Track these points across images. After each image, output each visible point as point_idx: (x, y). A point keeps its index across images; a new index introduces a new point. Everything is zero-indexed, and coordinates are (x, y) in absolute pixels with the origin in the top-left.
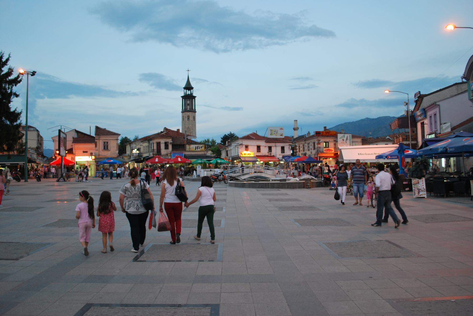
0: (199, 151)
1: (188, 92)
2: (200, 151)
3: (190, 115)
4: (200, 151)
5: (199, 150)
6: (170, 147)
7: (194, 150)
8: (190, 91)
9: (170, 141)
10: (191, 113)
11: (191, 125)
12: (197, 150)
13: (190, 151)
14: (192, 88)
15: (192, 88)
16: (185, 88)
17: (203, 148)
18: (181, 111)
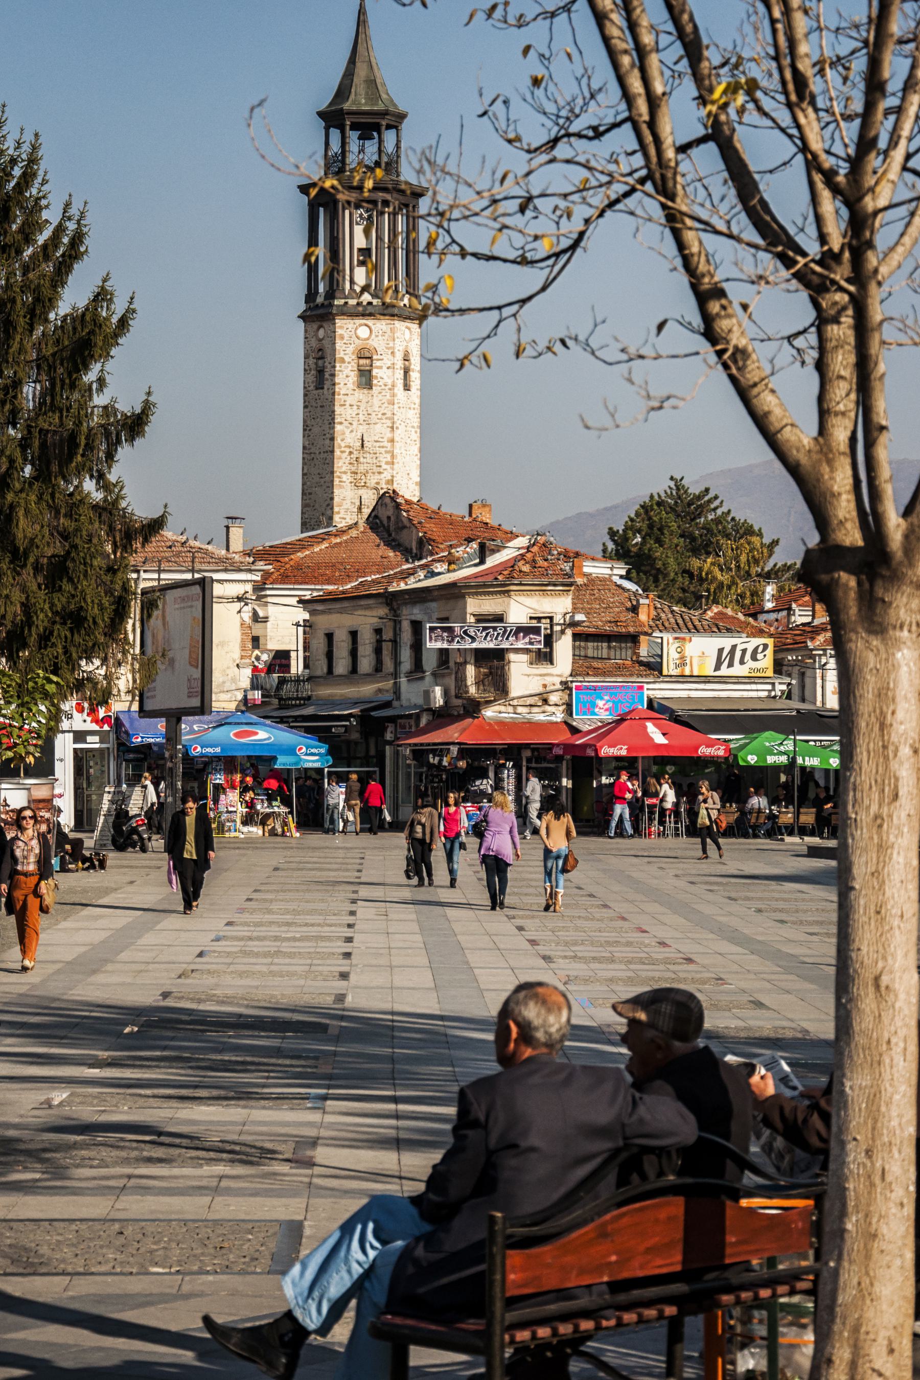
0: (738, 680)
1: (361, 152)
2: (750, 679)
3: (377, 343)
4: (750, 679)
5: (738, 670)
6: (564, 647)
7: (709, 671)
8: (371, 148)
9: (559, 606)
10: (381, 325)
11: (380, 430)
12: (724, 671)
13: (682, 678)
14: (395, 120)
15: (395, 120)
16: (332, 118)
17: (766, 662)
18: (302, 307)
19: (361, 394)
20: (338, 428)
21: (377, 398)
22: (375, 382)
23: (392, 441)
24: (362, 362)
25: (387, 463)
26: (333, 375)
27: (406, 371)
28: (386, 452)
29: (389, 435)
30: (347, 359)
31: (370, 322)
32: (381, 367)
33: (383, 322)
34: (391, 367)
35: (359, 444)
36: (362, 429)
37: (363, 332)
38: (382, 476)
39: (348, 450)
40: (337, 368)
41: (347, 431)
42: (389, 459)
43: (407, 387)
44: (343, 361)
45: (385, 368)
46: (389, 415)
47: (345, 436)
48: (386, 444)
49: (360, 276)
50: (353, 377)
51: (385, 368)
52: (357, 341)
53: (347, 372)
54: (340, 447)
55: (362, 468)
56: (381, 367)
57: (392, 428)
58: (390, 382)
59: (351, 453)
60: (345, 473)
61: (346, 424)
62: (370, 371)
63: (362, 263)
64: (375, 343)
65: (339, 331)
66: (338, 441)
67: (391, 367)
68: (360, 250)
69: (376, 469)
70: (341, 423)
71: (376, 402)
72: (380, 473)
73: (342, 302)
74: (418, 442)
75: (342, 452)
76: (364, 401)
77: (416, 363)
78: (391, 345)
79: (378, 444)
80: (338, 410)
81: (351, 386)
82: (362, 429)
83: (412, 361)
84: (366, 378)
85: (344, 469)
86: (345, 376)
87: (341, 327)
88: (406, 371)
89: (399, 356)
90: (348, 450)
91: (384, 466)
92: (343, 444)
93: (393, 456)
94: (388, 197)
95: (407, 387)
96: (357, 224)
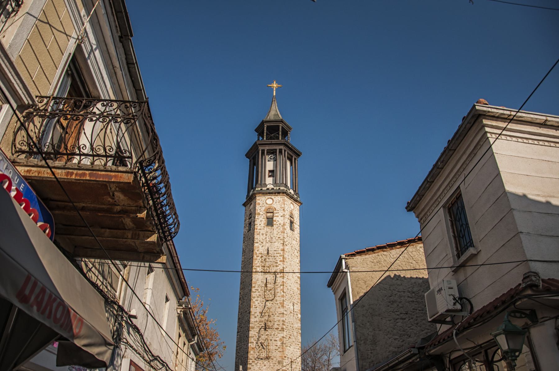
3: (276, 206)
11: (278, 245)
19: (268, 229)
20: (256, 245)
21: (276, 230)
22: (275, 223)
23: (283, 250)
24: (269, 214)
25: (280, 261)
26: (254, 221)
27: (292, 223)
28: (280, 256)
29: (282, 247)
30: (261, 213)
31: (273, 197)
32: (278, 216)
33: (279, 197)
34: (283, 216)
35: (266, 252)
36: (268, 245)
37: (269, 201)
38: (278, 268)
39: (260, 255)
40: (256, 217)
41: (260, 247)
42: (282, 259)
43: (292, 229)
44: (259, 214)
45: (280, 217)
46: (282, 238)
47: (259, 248)
48: (280, 252)
49: (269, 181)
50: (264, 221)
51: (280, 217)
52: (266, 205)
53: (261, 219)
54: (256, 254)
55: (267, 264)
56: (278, 216)
57: (283, 244)
58: (282, 223)
59: (262, 257)
60: (259, 267)
61: (260, 243)
62: (272, 218)
63: (269, 176)
64: (275, 206)
65: (258, 201)
66: (255, 251)
67: (283, 216)
68: (270, 171)
69: (275, 264)
70: (257, 243)
71: (275, 232)
72: (277, 266)
73: (259, 189)
74: (299, 257)
75: (257, 256)
76: (269, 232)
77: (297, 220)
78: (283, 206)
79: (276, 252)
80: (256, 236)
81: (262, 225)
82: (268, 245)
83: (295, 219)
84: (270, 222)
85: (258, 265)
86: (260, 221)
87: (259, 200)
88: (292, 223)
89: (288, 216)
90: (260, 255)
91: (279, 263)
92: (258, 253)
93: (284, 258)
94: (282, 147)
95: (292, 229)
96: (268, 161)
